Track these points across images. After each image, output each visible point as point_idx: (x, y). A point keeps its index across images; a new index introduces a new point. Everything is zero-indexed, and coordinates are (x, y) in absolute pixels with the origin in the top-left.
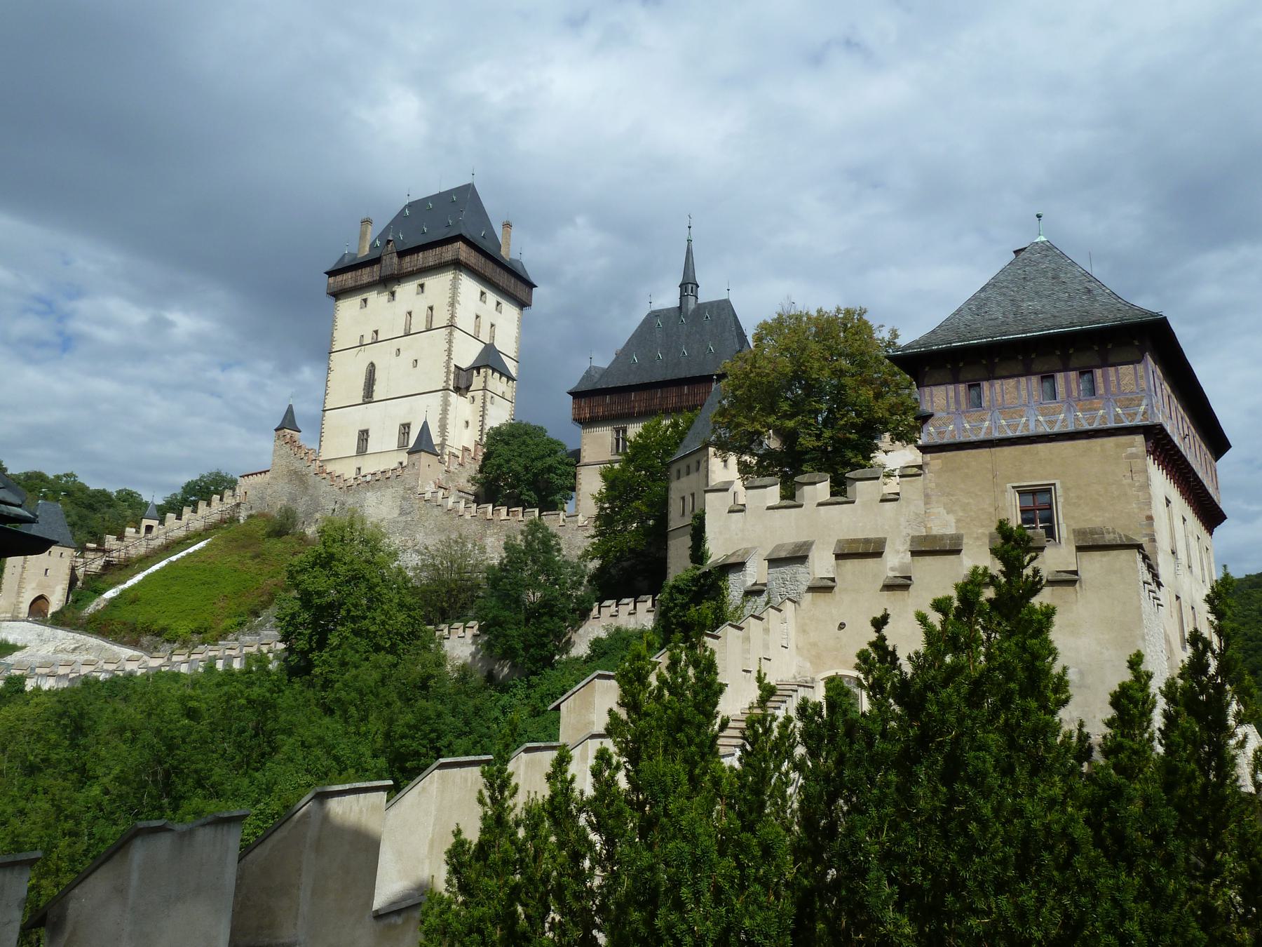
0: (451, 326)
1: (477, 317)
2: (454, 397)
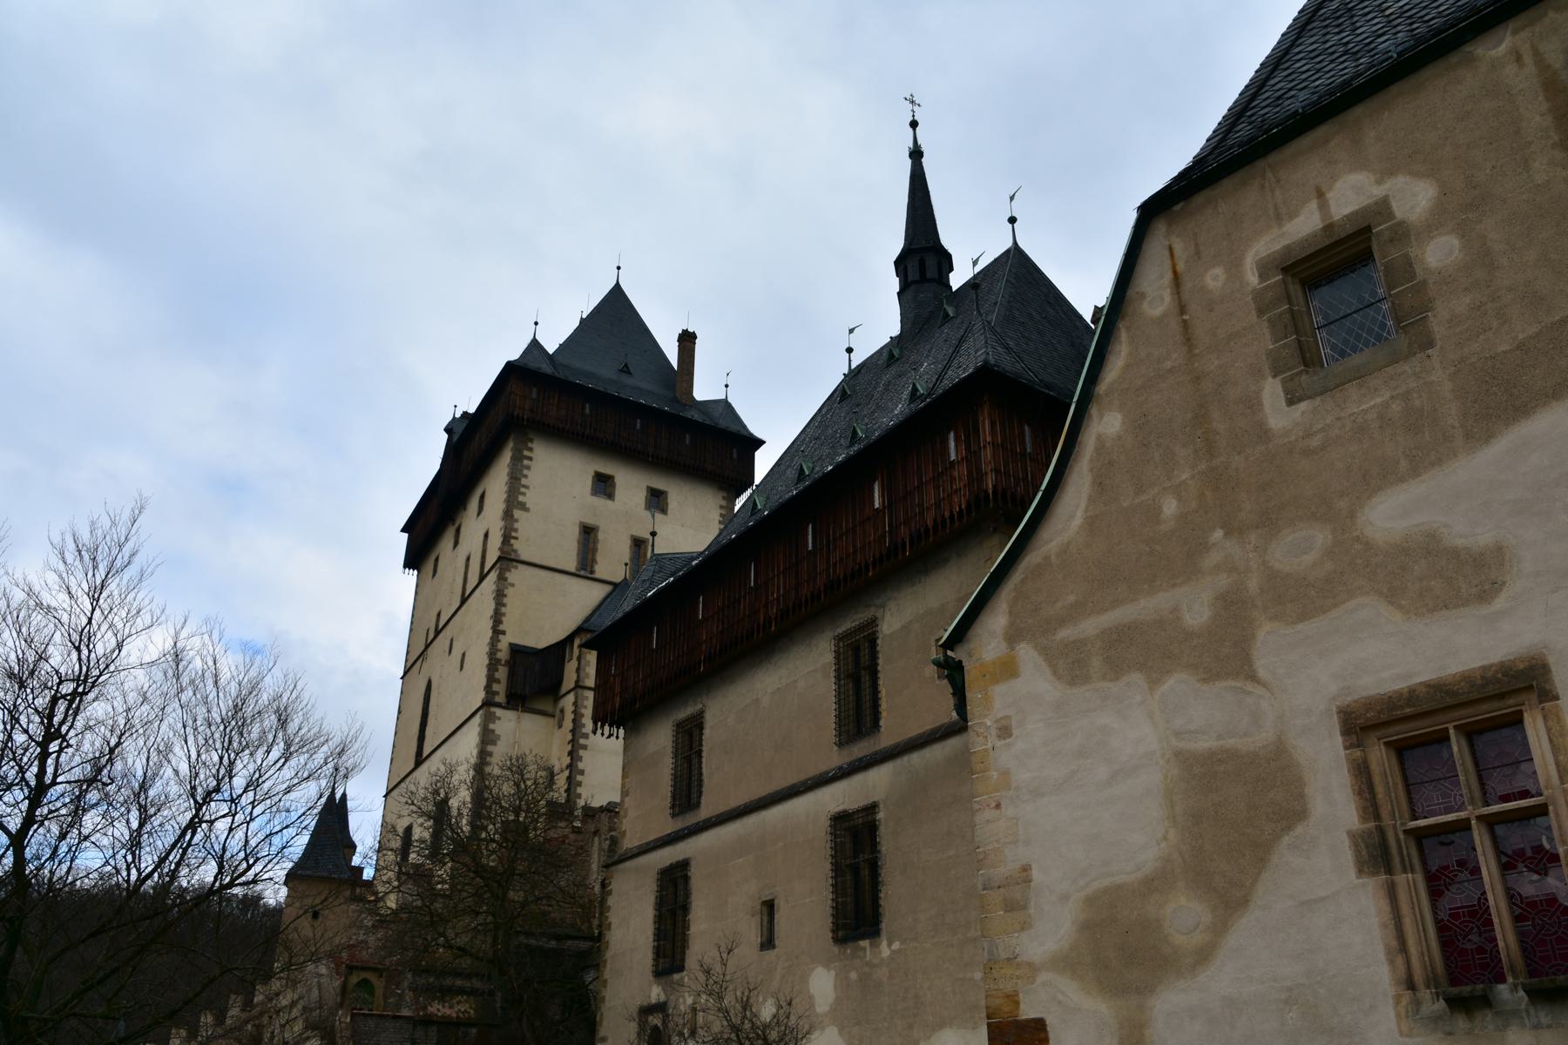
0: (508, 559)
1: (588, 533)
2: (507, 723)
